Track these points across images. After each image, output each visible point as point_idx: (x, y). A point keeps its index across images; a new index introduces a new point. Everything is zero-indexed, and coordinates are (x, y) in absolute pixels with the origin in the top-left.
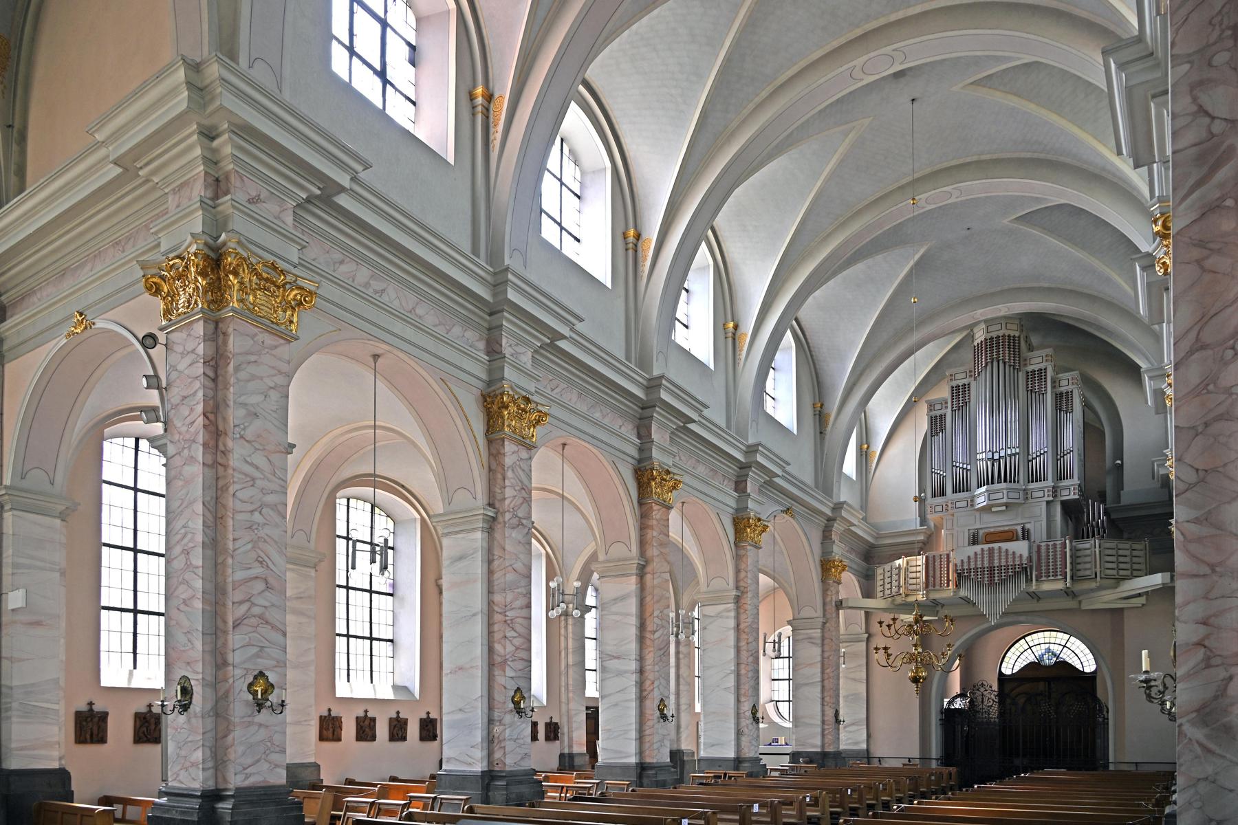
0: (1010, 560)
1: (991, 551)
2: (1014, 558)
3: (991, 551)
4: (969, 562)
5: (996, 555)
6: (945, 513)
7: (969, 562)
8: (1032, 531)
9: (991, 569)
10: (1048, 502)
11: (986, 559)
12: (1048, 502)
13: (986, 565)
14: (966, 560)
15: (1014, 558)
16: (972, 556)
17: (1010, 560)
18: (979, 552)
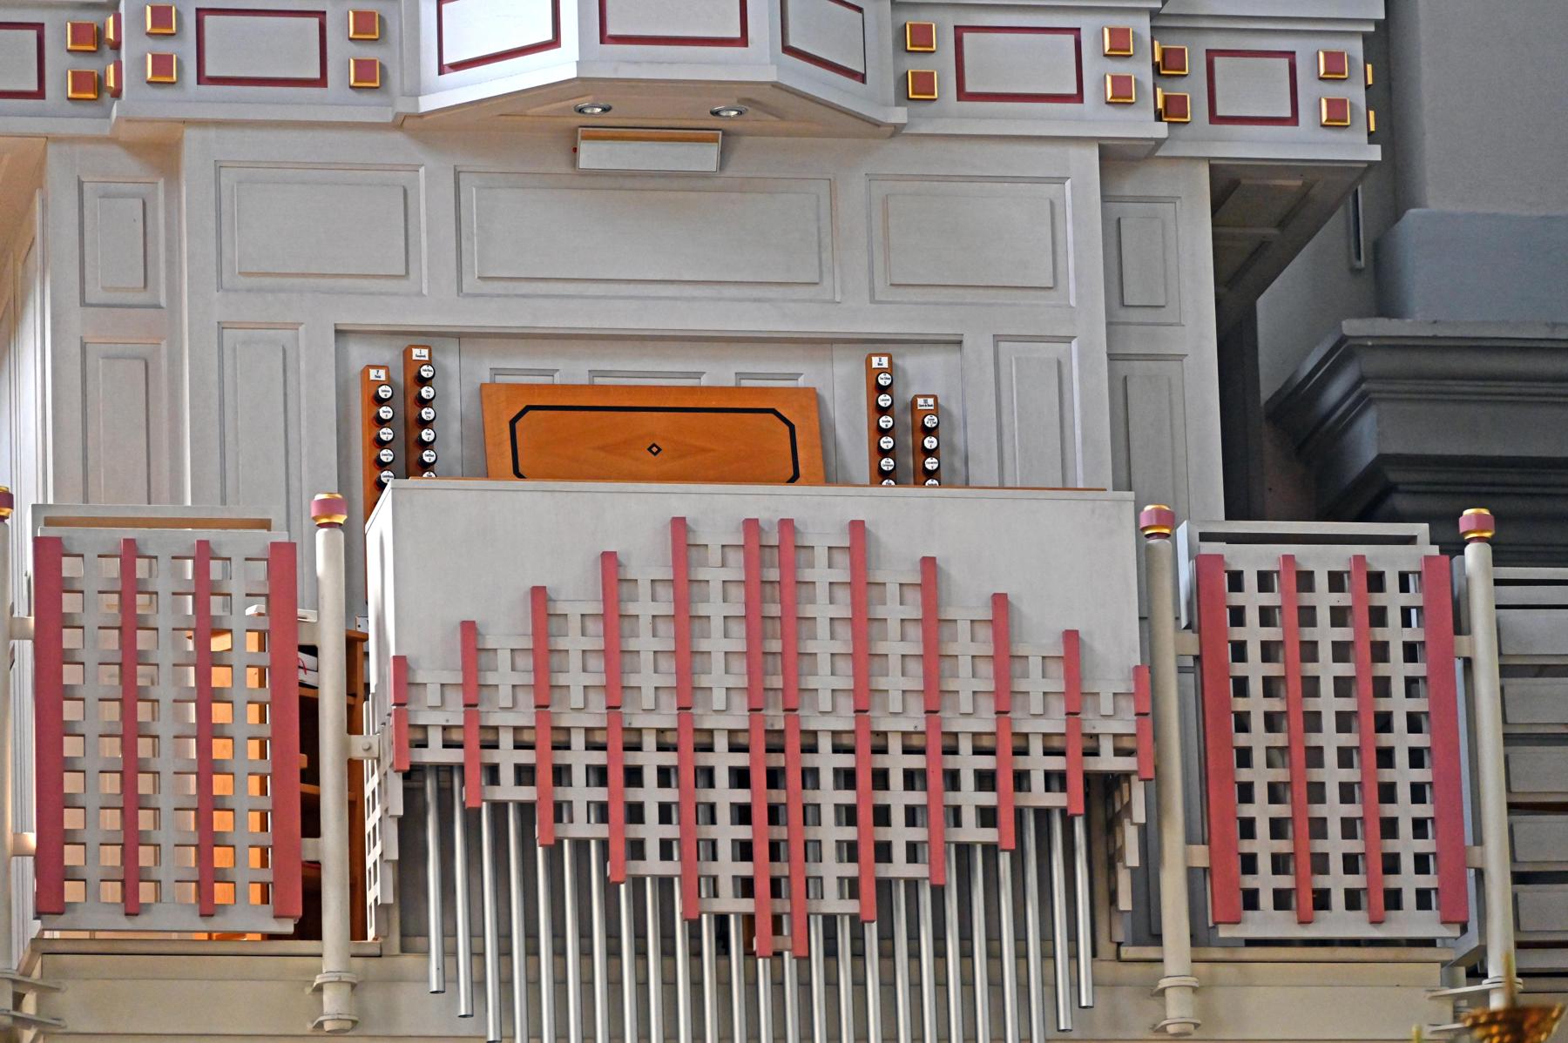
0: (969, 682)
1: (771, 556)
2: (1005, 660)
3: (771, 556)
4: (544, 655)
5: (825, 610)
6: (59, 117)
7: (544, 655)
8: (975, 437)
9: (775, 767)
10: (1116, 159)
11: (721, 642)
12: (1116, 159)
13: (723, 710)
14: (506, 633)
15: (1005, 660)
16: (578, 597)
17: (969, 682)
18: (648, 562)
